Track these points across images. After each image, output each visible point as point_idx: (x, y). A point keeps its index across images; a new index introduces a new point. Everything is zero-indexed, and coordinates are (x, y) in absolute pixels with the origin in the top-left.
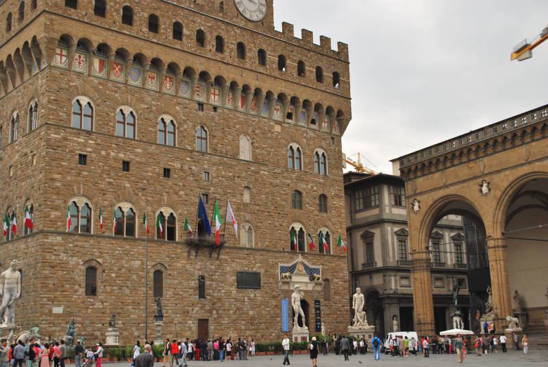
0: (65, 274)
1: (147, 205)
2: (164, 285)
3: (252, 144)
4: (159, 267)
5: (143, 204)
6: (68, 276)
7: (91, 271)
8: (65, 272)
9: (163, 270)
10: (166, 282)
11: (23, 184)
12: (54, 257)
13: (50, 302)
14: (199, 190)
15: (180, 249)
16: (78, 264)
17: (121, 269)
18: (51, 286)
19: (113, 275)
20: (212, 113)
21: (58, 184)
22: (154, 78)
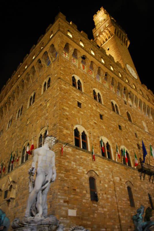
0: (76, 180)
1: (116, 142)
2: (134, 198)
3: (147, 126)
4: (129, 184)
5: (113, 141)
6: (78, 181)
7: (92, 181)
8: (76, 178)
9: (131, 186)
10: (135, 195)
11: (38, 122)
12: (67, 164)
13: (66, 204)
14: (135, 141)
15: (136, 173)
16: (83, 172)
17: (109, 182)
18: (66, 188)
19: (106, 186)
20: (130, 107)
21: (67, 113)
22: (105, 83)
